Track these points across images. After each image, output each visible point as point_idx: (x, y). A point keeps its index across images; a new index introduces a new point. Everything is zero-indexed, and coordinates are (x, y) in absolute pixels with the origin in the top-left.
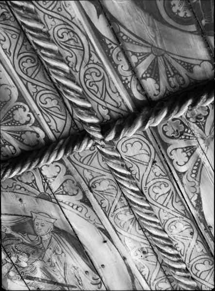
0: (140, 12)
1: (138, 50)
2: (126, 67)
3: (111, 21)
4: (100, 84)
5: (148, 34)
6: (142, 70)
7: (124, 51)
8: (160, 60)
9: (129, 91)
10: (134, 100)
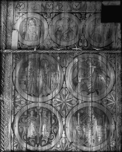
0: (19, 136)
1: (16, 141)
2: (13, 143)
3: (14, 135)
4: (7, 145)
5: (19, 139)
6: (15, 145)
7: (14, 141)
8: (18, 145)
9: (11, 148)
10: (11, 150)
